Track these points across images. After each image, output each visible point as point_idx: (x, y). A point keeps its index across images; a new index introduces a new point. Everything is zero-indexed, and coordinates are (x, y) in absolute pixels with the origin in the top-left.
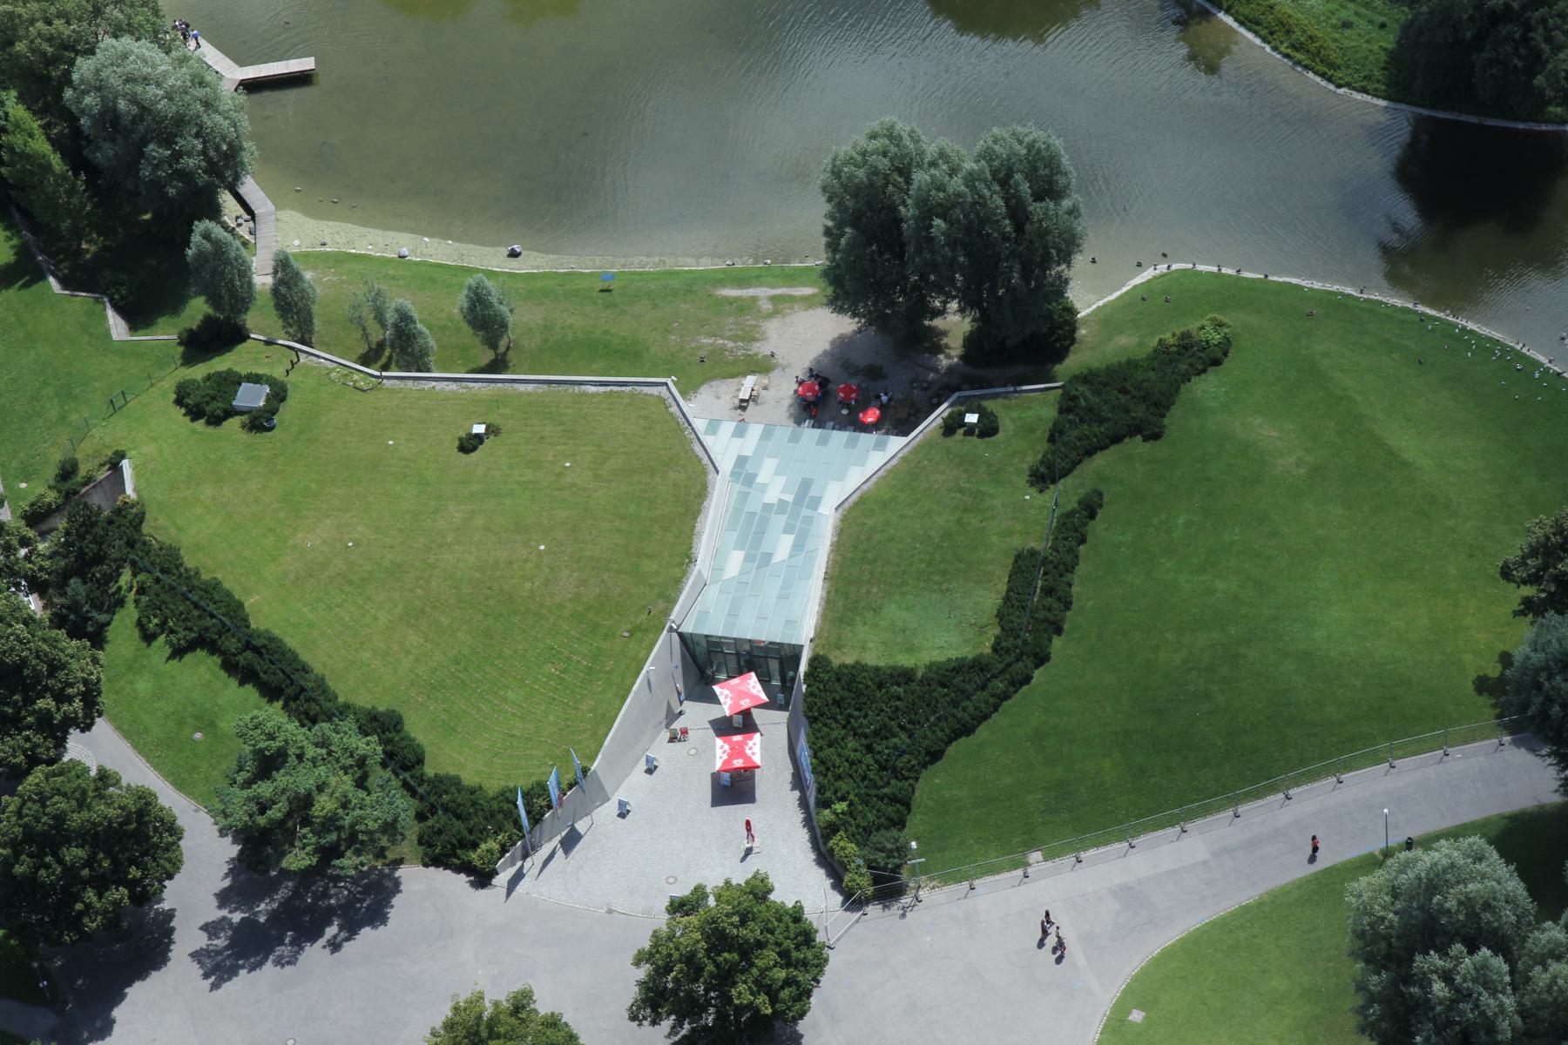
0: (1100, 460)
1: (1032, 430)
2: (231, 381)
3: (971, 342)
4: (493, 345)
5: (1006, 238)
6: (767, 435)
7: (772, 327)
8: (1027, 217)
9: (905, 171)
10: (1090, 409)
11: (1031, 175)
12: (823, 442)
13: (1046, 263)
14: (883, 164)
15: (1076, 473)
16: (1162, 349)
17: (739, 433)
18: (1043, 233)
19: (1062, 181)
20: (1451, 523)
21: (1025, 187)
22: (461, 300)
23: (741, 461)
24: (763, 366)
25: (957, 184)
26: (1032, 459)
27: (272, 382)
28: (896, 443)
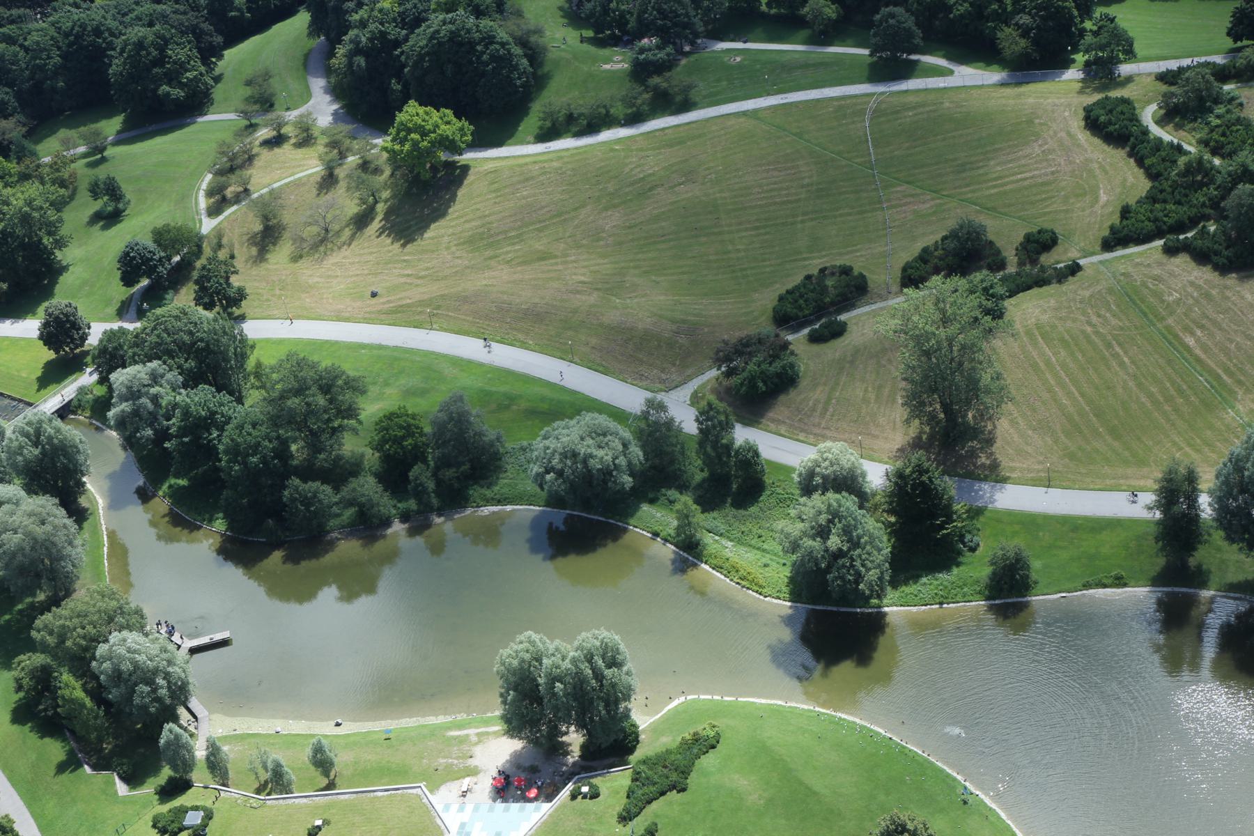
0: (655, 805)
1: (618, 793)
2: (183, 811)
3: (584, 747)
4: (326, 773)
5: (594, 690)
6: (476, 809)
7: (477, 750)
8: (603, 677)
9: (539, 660)
10: (648, 778)
11: (603, 657)
12: (506, 810)
13: (617, 702)
14: (527, 656)
15: (642, 814)
16: (684, 742)
17: (461, 810)
18: (613, 685)
19: (620, 657)
20: (842, 823)
21: (600, 663)
22: (308, 751)
23: (463, 825)
24: (473, 772)
25: (567, 665)
26: (619, 808)
27: (205, 809)
28: (545, 808)
